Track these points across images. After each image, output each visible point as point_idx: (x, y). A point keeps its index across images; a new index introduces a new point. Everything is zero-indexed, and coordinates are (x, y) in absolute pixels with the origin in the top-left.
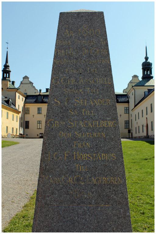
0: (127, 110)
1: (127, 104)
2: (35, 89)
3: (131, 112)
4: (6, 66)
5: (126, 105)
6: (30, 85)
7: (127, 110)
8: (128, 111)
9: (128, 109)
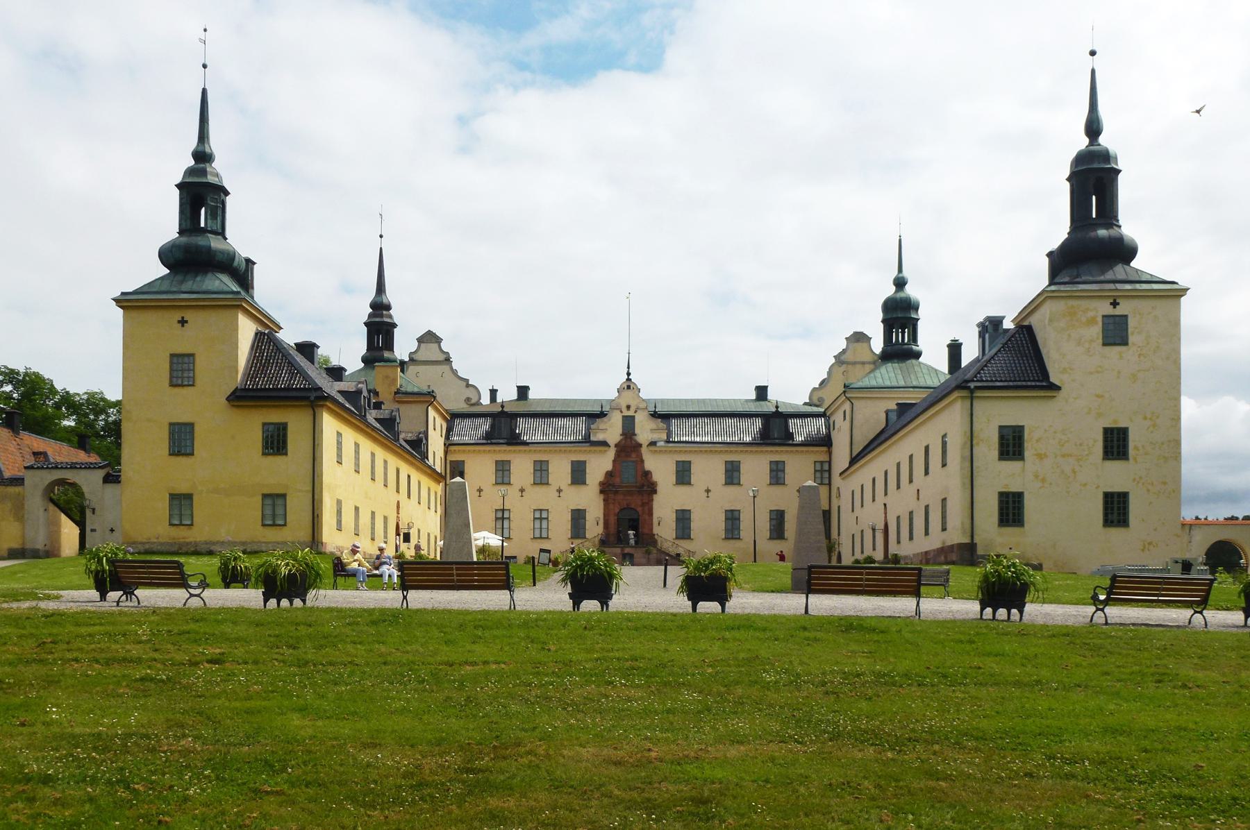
0: (822, 471)
1: (825, 449)
2: (468, 385)
3: (837, 480)
4: (380, 307)
5: (819, 454)
6: (445, 368)
7: (824, 472)
8: (826, 475)
9: (826, 467)
